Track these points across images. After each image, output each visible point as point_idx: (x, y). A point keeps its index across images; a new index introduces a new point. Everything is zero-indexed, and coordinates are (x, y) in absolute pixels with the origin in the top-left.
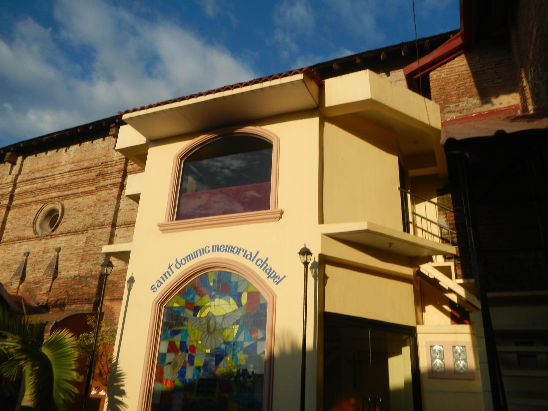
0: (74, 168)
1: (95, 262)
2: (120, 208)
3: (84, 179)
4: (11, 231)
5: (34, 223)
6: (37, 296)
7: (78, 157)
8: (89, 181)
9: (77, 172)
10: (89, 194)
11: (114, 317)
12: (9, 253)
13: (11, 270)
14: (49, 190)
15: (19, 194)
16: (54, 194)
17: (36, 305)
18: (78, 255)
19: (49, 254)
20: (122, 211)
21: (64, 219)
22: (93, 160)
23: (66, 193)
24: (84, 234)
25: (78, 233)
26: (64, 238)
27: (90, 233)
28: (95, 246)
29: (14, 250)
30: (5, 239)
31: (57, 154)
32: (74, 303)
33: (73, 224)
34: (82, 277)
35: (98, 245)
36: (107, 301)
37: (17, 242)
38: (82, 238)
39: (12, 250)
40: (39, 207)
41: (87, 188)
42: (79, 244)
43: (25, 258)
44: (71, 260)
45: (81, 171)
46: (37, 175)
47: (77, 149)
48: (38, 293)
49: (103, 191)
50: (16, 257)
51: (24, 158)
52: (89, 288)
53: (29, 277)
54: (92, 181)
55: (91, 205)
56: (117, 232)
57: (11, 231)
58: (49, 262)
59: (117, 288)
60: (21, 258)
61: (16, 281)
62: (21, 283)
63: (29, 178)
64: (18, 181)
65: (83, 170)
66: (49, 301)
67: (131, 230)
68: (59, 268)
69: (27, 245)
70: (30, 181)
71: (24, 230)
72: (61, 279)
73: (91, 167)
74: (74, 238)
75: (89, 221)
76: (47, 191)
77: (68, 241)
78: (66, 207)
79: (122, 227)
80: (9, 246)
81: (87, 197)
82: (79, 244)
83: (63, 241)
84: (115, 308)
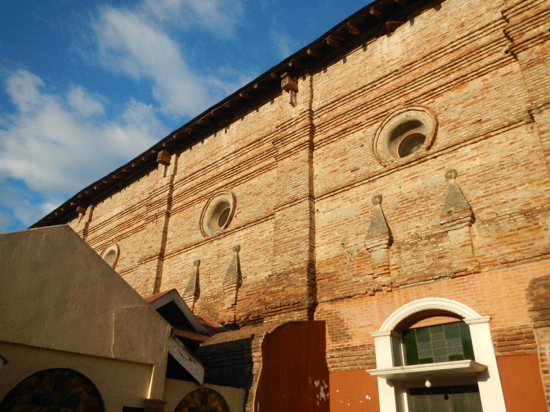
1: (295, 251)
2: (315, 174)
4: (175, 241)
5: (201, 223)
6: (220, 313)
7: (242, 133)
8: (262, 154)
9: (244, 149)
10: (266, 171)
11: (344, 327)
12: (175, 267)
13: (181, 286)
14: (213, 181)
15: (178, 196)
17: (221, 326)
18: (265, 249)
19: (225, 257)
20: (318, 177)
21: (238, 209)
22: (262, 129)
23: (235, 178)
24: (269, 221)
26: (242, 233)
27: (279, 215)
29: (181, 262)
30: (168, 252)
31: (216, 138)
32: (276, 313)
34: (281, 274)
35: (295, 228)
36: (326, 304)
37: (183, 251)
38: (268, 226)
39: (177, 263)
40: (203, 204)
43: (196, 267)
44: (258, 258)
45: (250, 146)
46: (195, 169)
47: (239, 125)
48: (220, 309)
50: (184, 270)
51: (178, 156)
52: (295, 288)
53: (205, 291)
55: (271, 182)
56: (317, 206)
57: (175, 241)
58: (228, 266)
59: (337, 283)
60: (191, 270)
61: (190, 298)
62: (195, 301)
63: (187, 175)
64: (174, 182)
66: (237, 318)
67: (340, 198)
68: (242, 272)
69: (196, 252)
70: (189, 178)
71: (189, 235)
72: (247, 285)
73: (262, 138)
74: (256, 229)
75: (273, 202)
76: (210, 183)
77: (249, 236)
78: (237, 194)
79: (323, 197)
80: (174, 258)
81: (263, 175)
82: (264, 236)
84: (342, 313)
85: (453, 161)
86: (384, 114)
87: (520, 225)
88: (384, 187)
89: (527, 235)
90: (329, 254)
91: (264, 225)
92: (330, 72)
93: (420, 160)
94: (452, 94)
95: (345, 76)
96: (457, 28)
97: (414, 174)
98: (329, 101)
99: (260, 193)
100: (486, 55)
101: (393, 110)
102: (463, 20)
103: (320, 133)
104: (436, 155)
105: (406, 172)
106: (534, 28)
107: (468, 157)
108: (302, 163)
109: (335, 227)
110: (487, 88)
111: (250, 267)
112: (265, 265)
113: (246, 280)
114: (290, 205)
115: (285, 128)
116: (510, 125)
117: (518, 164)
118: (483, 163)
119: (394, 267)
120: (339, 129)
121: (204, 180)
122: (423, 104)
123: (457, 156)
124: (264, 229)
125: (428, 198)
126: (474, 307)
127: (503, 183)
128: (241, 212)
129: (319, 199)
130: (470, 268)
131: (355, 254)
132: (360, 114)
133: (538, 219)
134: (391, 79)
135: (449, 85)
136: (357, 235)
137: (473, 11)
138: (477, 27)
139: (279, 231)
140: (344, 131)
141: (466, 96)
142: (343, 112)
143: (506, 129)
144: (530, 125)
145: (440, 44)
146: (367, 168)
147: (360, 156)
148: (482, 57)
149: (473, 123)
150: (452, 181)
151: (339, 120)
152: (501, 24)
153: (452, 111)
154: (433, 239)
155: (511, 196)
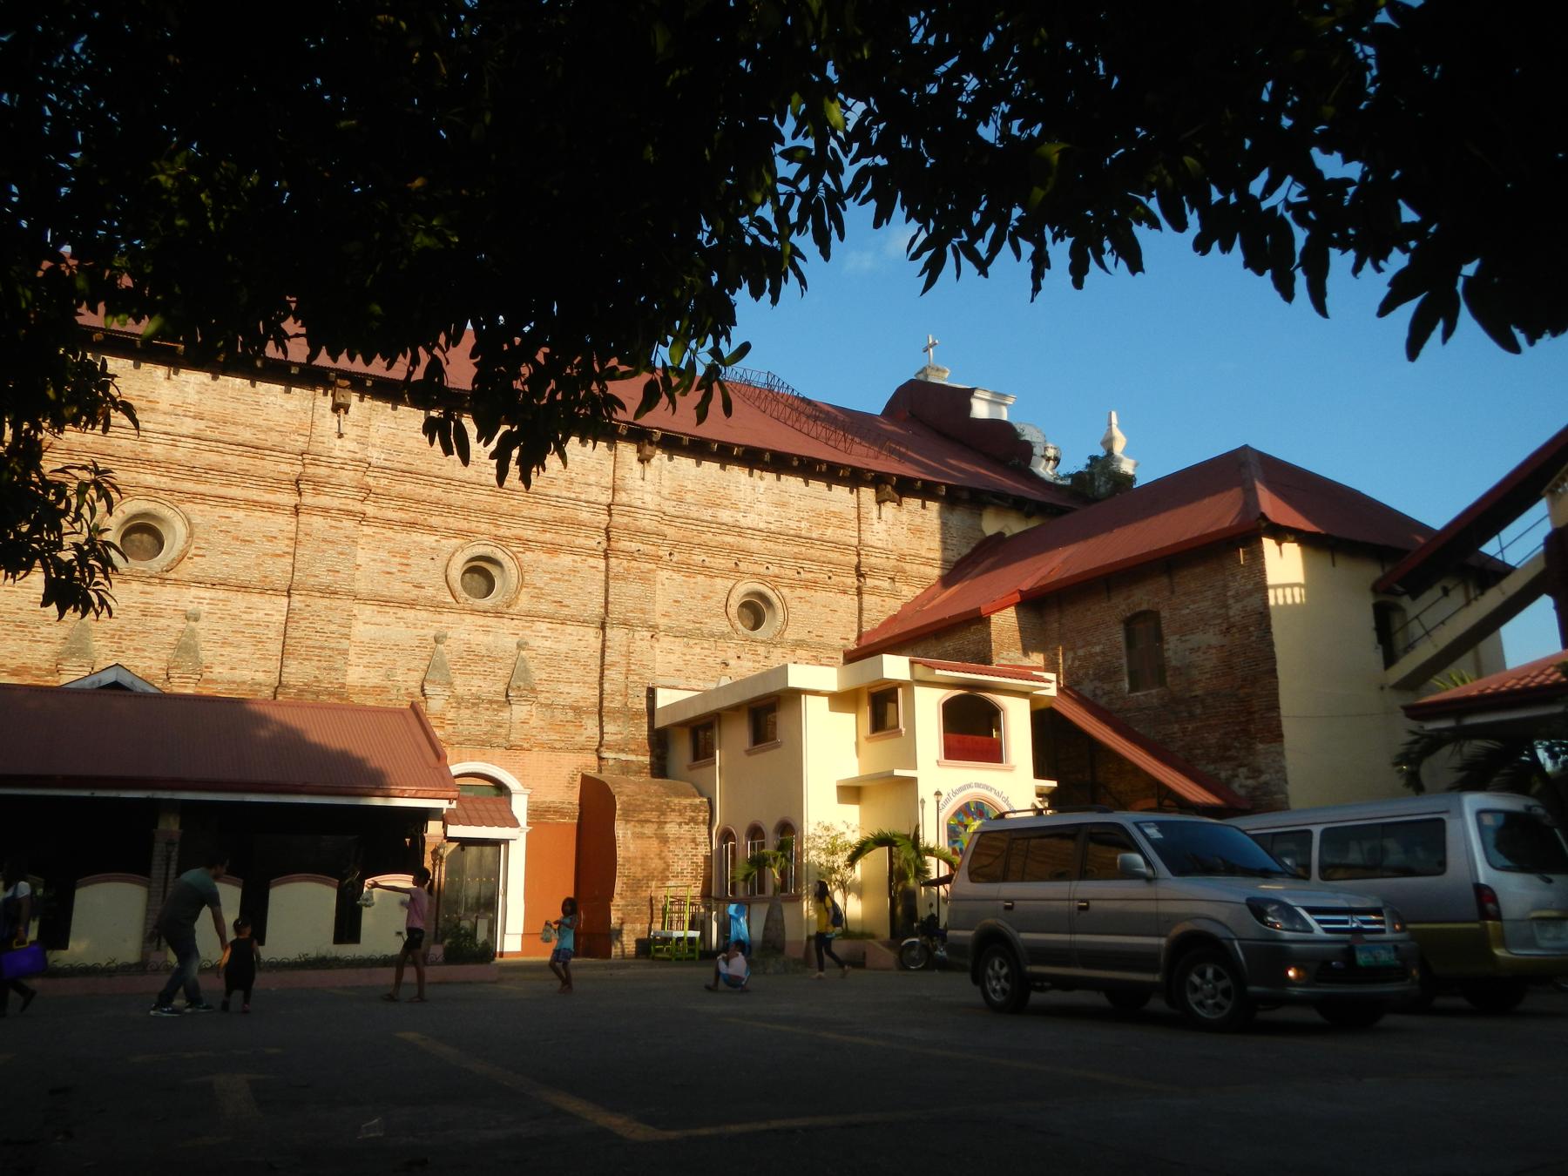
1: (325, 664)
3: (248, 470)
9: (221, 445)
14: (133, 465)
16: (150, 479)
18: (255, 637)
19: (162, 622)
23: (189, 486)
24: (267, 596)
25: (249, 590)
26: (208, 594)
28: (316, 632)
29: (30, 588)
33: (227, 566)
35: (325, 631)
41: (255, 491)
42: (254, 616)
44: (238, 646)
47: (204, 383)
49: (315, 517)
54: (276, 484)
61: (80, 669)
65: (241, 448)
74: (239, 601)
77: (221, 603)
78: (196, 520)
79: (368, 602)
81: (257, 513)
83: (204, 599)
85: (528, 632)
86: (469, 534)
87: (569, 718)
88: (451, 625)
89: (571, 729)
90: (366, 681)
92: (401, 416)
93: (498, 614)
94: (544, 557)
96: (566, 481)
97: (488, 627)
98: (396, 465)
99: (248, 541)
100: (583, 535)
102: (573, 475)
103: (373, 504)
104: (514, 617)
105: (481, 620)
106: (629, 541)
107: (543, 634)
108: (345, 540)
109: (379, 648)
110: (574, 571)
111: (222, 655)
112: (254, 661)
113: (211, 672)
114: (322, 595)
115: (317, 462)
116: (584, 622)
117: (579, 661)
118: (553, 647)
119: (449, 722)
121: (110, 452)
122: (513, 548)
123: (534, 628)
124: (255, 606)
125: (495, 660)
126: (519, 779)
127: (564, 675)
128: (204, 556)
129: (361, 602)
130: (526, 745)
132: (437, 513)
133: (582, 719)
134: (484, 492)
135: (544, 545)
136: (408, 670)
137: (584, 472)
138: (583, 497)
139: (298, 625)
142: (416, 497)
143: (580, 624)
144: (597, 630)
145: (545, 487)
146: (435, 592)
147: (428, 571)
148: (580, 535)
149: (555, 602)
150: (523, 653)
151: (407, 504)
152: (603, 510)
153: (540, 577)
154: (495, 706)
155: (567, 690)
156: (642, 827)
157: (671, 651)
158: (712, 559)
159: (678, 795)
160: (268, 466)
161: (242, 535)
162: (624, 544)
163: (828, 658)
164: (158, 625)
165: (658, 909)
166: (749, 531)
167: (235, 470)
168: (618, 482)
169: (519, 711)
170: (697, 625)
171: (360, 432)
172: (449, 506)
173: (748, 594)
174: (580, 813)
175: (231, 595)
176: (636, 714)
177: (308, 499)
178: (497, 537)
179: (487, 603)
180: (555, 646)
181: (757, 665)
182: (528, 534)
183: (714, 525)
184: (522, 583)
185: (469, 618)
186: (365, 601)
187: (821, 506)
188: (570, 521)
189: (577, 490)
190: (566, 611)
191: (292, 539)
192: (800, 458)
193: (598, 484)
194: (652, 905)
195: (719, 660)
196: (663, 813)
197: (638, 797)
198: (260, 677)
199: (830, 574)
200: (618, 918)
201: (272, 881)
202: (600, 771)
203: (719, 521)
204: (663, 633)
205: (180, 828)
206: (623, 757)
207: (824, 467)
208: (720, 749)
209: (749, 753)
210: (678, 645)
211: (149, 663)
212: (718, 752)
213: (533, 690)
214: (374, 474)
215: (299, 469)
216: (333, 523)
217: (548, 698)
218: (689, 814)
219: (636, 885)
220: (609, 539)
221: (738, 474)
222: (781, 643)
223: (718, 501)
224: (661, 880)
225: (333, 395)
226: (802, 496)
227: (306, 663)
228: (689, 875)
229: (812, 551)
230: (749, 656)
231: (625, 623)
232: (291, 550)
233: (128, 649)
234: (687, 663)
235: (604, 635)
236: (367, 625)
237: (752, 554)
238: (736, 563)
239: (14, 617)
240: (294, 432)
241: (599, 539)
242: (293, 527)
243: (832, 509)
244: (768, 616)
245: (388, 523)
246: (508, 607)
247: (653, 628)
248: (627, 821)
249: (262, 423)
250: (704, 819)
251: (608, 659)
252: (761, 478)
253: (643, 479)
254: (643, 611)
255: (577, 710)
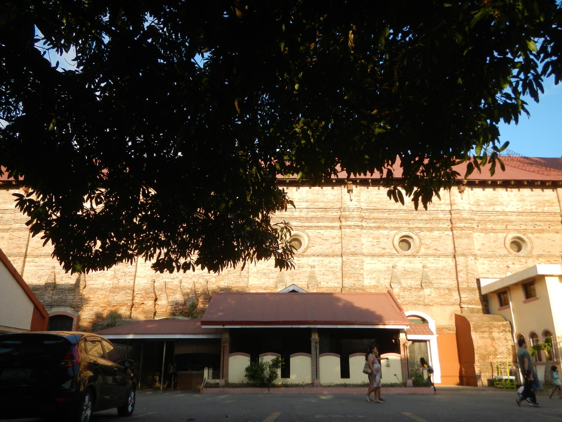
0: (311, 206)
19: (304, 269)
27: (345, 258)
33: (321, 249)
49: (347, 229)
50: (269, 268)
54: (333, 220)
65: (321, 209)
72: (322, 287)
74: (326, 260)
78: (310, 235)
85: (426, 261)
87: (446, 293)
89: (447, 296)
91: (331, 259)
93: (414, 256)
94: (428, 233)
95: (379, 198)
97: (411, 261)
98: (371, 208)
101: (403, 228)
105: (407, 259)
116: (447, 256)
120: (374, 225)
121: (283, 217)
125: (415, 273)
127: (442, 276)
130: (431, 304)
131: (384, 287)
132: (387, 222)
134: (403, 213)
138: (439, 209)
140: (379, 228)
141: (433, 237)
150: (425, 269)
151: (376, 221)
154: (417, 290)
156: (483, 334)
157: (484, 264)
158: (495, 226)
159: (496, 320)
160: (329, 214)
161: (325, 238)
162: (459, 225)
163: (554, 260)
164: (303, 271)
165: (495, 367)
166: (510, 213)
167: (320, 217)
168: (452, 202)
169: (427, 291)
170: (494, 253)
171: (357, 198)
172: (391, 219)
173: (513, 238)
174: (457, 329)
175: (324, 258)
176: (473, 289)
177: (344, 223)
178: (409, 228)
179: (409, 252)
180: (437, 266)
181: (522, 266)
182: (421, 225)
183: (494, 213)
184: (421, 244)
185: (404, 259)
186: (367, 256)
187: (540, 198)
188: (436, 219)
189: (437, 207)
190: (439, 252)
191: (340, 237)
192: (528, 181)
193: (444, 204)
194: (492, 365)
195: (505, 266)
196: (491, 328)
197: (479, 322)
198: (336, 285)
199: (549, 226)
200: (478, 371)
201: (350, 355)
202: (462, 312)
203: (496, 210)
204: (479, 257)
205: (319, 337)
206: (470, 306)
207: (539, 183)
208: (511, 301)
209: (524, 302)
210: (486, 261)
211: (302, 283)
212: (510, 303)
213: (431, 283)
214: (364, 212)
215: (339, 214)
216: (353, 230)
217: (437, 286)
218: (502, 328)
219: (484, 357)
220: (452, 223)
221: (501, 192)
222: (531, 256)
223: (494, 203)
224: (494, 355)
225: (347, 187)
226: (531, 196)
227: (350, 279)
228: (506, 353)
229: (539, 217)
230: (518, 263)
231: (464, 255)
232: (340, 241)
233: (295, 279)
234: (491, 268)
235: (456, 260)
236: (369, 264)
237: (512, 222)
238: (506, 227)
239: (264, 272)
240: (336, 202)
241: (448, 224)
242: (340, 233)
243: (546, 199)
244: (524, 246)
245: (371, 228)
246: (417, 253)
247: (475, 255)
248: (476, 332)
249: (326, 200)
250: (509, 330)
251: (458, 269)
252: (512, 191)
253: (462, 199)
254: (470, 249)
255: (449, 289)
